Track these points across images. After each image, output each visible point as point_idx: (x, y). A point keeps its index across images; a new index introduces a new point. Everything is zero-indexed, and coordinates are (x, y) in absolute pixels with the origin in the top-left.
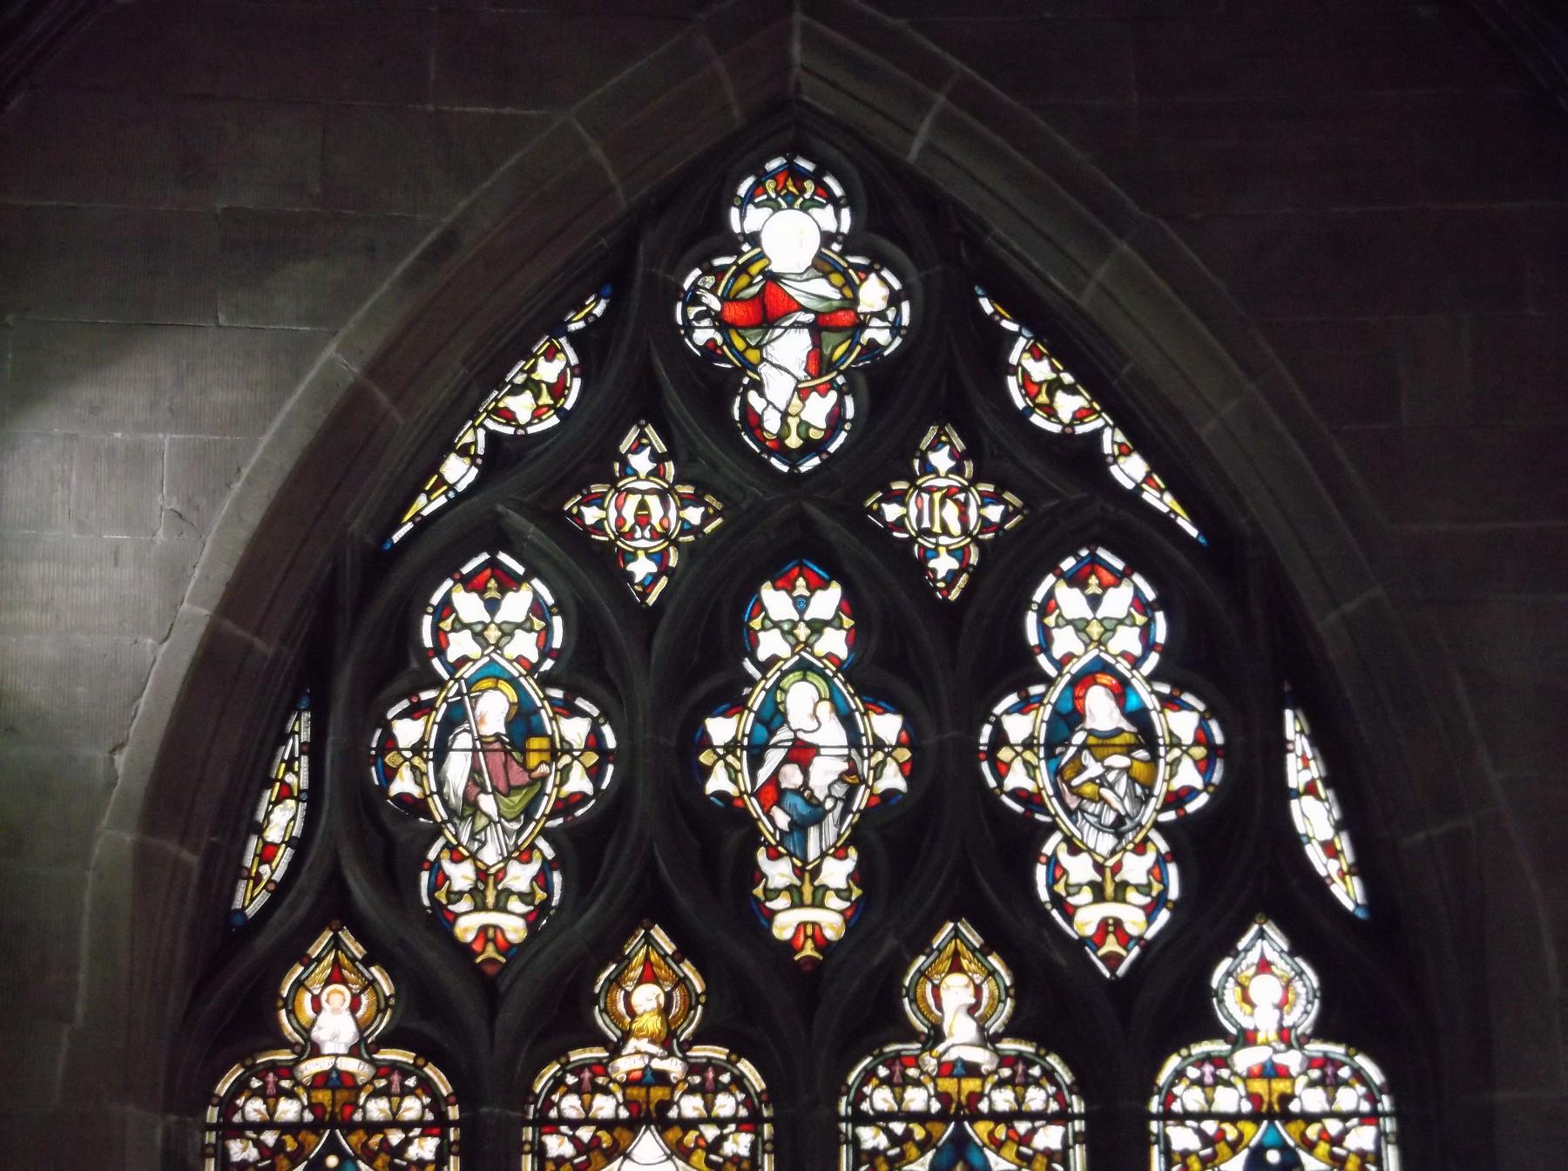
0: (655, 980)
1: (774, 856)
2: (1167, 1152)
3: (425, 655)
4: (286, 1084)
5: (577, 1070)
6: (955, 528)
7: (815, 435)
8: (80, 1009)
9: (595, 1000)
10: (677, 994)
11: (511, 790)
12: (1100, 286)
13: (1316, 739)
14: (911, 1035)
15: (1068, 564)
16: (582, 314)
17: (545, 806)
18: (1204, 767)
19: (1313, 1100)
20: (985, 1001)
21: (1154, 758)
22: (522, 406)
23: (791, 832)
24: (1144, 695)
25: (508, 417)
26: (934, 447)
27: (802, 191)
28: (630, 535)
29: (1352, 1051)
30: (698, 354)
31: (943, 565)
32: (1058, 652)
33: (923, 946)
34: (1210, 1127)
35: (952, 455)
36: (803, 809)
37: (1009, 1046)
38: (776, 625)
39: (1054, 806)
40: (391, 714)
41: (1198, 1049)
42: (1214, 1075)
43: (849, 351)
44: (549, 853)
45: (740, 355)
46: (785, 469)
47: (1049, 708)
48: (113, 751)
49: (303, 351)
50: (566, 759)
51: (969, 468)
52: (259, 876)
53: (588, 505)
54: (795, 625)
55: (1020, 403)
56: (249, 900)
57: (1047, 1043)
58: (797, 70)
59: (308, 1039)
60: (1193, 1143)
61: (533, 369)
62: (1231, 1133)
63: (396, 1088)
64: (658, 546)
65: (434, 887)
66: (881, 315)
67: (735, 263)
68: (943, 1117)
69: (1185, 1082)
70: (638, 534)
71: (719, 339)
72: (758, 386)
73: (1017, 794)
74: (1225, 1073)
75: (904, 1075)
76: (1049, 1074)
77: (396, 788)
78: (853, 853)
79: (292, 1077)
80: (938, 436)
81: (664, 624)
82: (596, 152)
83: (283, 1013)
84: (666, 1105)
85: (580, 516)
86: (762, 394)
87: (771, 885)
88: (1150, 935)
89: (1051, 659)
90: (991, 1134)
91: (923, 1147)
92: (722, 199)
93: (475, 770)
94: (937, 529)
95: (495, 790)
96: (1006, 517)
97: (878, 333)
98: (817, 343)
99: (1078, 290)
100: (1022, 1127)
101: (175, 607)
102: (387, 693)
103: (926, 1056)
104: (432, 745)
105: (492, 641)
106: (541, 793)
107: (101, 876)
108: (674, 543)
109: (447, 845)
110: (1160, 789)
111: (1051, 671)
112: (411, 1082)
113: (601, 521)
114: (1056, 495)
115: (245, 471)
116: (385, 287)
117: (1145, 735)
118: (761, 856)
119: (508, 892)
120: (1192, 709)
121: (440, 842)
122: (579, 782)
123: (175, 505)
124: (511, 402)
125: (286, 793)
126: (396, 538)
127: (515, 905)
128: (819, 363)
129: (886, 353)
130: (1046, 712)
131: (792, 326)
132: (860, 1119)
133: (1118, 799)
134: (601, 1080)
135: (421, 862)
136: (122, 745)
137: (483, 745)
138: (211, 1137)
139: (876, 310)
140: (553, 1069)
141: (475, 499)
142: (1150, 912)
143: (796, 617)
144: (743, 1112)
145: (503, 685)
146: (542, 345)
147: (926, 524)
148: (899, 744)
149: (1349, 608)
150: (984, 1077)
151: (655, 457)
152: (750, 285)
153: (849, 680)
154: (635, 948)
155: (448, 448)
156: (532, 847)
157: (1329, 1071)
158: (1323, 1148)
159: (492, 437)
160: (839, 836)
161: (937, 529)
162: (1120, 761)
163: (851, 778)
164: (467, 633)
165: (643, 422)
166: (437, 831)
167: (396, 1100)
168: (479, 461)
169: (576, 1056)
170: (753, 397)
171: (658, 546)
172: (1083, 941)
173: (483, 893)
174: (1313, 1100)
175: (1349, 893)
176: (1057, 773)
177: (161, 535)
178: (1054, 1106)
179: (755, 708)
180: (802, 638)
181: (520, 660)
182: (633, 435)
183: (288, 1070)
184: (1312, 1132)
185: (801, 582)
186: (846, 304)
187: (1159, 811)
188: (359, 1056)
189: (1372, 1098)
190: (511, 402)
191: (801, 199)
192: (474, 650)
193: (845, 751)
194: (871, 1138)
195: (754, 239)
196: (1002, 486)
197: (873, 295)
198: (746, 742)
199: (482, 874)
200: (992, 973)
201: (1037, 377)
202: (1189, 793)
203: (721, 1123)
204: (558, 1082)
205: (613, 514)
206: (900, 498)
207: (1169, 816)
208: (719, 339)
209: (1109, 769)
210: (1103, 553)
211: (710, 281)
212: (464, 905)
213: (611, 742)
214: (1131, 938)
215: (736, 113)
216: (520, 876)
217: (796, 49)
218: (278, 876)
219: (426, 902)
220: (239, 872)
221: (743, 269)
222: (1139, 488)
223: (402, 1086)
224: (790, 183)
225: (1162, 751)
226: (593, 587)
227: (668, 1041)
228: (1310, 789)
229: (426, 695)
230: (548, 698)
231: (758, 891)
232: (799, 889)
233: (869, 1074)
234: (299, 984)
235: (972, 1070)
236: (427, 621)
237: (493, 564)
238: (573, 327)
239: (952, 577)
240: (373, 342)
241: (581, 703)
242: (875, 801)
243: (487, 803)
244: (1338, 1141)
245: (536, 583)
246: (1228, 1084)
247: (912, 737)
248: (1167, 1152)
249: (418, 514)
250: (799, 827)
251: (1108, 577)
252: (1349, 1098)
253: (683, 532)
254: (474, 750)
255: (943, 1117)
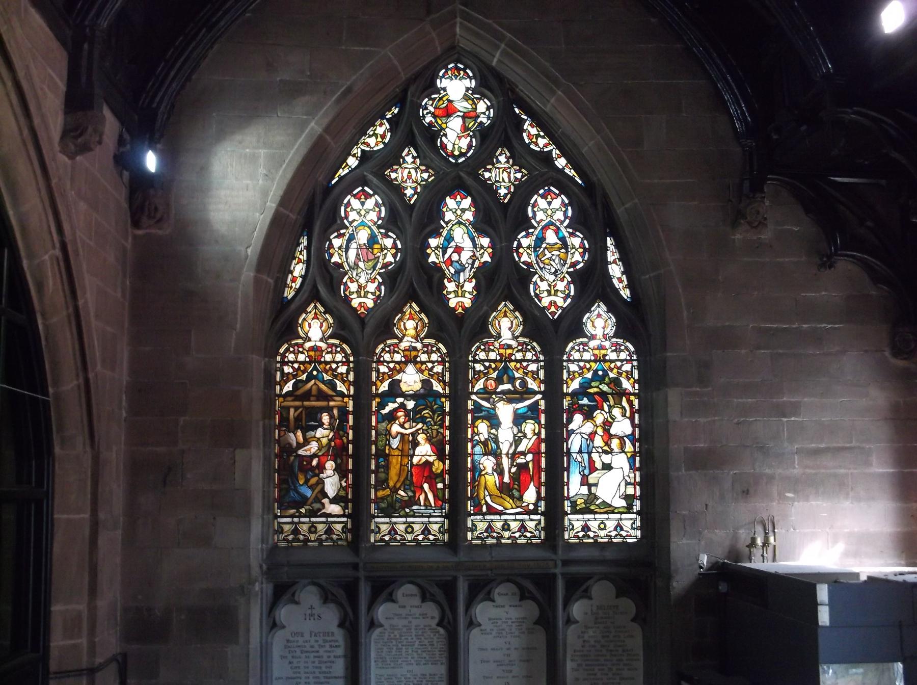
0: (413, 319)
1: (450, 281)
2: (569, 372)
3: (342, 219)
4: (301, 349)
5: (389, 347)
6: (507, 180)
7: (463, 151)
8: (238, 326)
9: (395, 325)
10: (420, 323)
11: (369, 260)
12: (553, 106)
13: (616, 246)
14: (492, 336)
15: (541, 191)
16: (391, 113)
17: (379, 266)
18: (582, 255)
19: (613, 356)
20: (514, 326)
21: (567, 252)
22: (372, 141)
23: (455, 274)
24: (564, 232)
25: (368, 145)
26: (500, 155)
27: (460, 74)
28: (406, 182)
29: (625, 341)
31: (503, 191)
32: (538, 219)
33: (495, 309)
34: (582, 364)
35: (506, 157)
36: (459, 267)
37: (521, 339)
38: (451, 210)
39: (536, 266)
40: (331, 237)
41: (578, 341)
42: (583, 348)
43: (474, 124)
44: (381, 280)
45: (440, 126)
46: (454, 161)
47: (535, 236)
48: (247, 248)
49: (303, 125)
50: (385, 251)
51: (511, 161)
52: (292, 287)
53: (392, 172)
54: (456, 210)
55: (527, 141)
56: (289, 294)
57: (533, 339)
58: (458, 36)
59: (307, 336)
60: (577, 369)
61: (375, 130)
62: (588, 366)
63: (334, 351)
64: (414, 185)
65: (345, 290)
66: (484, 113)
68: (501, 361)
69: (575, 350)
70: (408, 181)
71: (434, 121)
72: (445, 135)
73: (524, 263)
74: (586, 348)
75: (489, 348)
76: (533, 348)
77: (333, 260)
78: (474, 281)
79: (303, 348)
80: (501, 151)
81: (416, 208)
82: (396, 62)
83: (299, 328)
84: (416, 357)
85: (390, 175)
86: (447, 138)
87: (449, 290)
88: (564, 306)
89: (536, 221)
90: (515, 366)
91: (494, 370)
92: (434, 77)
93: (358, 254)
94: (501, 180)
95: (364, 260)
96: (523, 177)
97: (483, 119)
98: (464, 122)
99: (545, 105)
100: (525, 364)
101: (265, 204)
102: (331, 230)
103: (496, 342)
104: (344, 247)
105: (363, 214)
106: (378, 262)
107: (244, 286)
108: (419, 184)
109: (349, 277)
110: (569, 261)
111: (536, 225)
112: (339, 349)
113: (396, 178)
114: (537, 170)
115: (287, 161)
116: (329, 104)
117: (565, 245)
118: (446, 281)
119: (368, 292)
120: (579, 237)
121: (347, 277)
122: (390, 258)
123: (265, 172)
124: (369, 140)
125: (300, 261)
126: (333, 182)
127: (370, 296)
128: (465, 128)
130: (534, 238)
132: (475, 361)
133: (556, 264)
134: (396, 349)
135: (341, 282)
136: (249, 246)
137: (360, 247)
138: (278, 365)
140: (382, 346)
141: (357, 170)
142: (565, 300)
143: (457, 208)
144: (440, 359)
145: (366, 228)
146: (378, 123)
147: (497, 179)
148: (489, 247)
149: (627, 206)
150: (513, 349)
151: (413, 157)
152: (443, 104)
153: (473, 227)
154: (407, 309)
155: (349, 154)
156: (375, 278)
157: (618, 347)
158: (615, 370)
159: (363, 151)
160: (470, 275)
161: (501, 180)
162: (557, 253)
163: (474, 258)
164: (355, 212)
166: (346, 273)
167: (334, 355)
168: (359, 159)
169: (389, 342)
170: (444, 138)
171: (414, 185)
172: (544, 308)
173: (360, 292)
174: (613, 356)
175: (626, 294)
176: (538, 256)
177: (261, 182)
178: (534, 358)
179: (444, 236)
180: (459, 214)
181: (371, 220)
182: (406, 150)
183: (301, 346)
184: (612, 365)
185: (458, 197)
187: (568, 268)
188: (323, 342)
189: (630, 355)
190: (369, 140)
192: (357, 217)
193: (472, 249)
194: (479, 367)
195: (444, 89)
196: (521, 167)
197: (482, 107)
198: (441, 246)
199: (360, 287)
200: (516, 317)
201: (532, 133)
202: (578, 262)
203: (433, 362)
204: (383, 350)
205: (400, 175)
206: (490, 171)
207: (572, 270)
208: (434, 121)
209: (553, 255)
210: (552, 188)
211: (431, 102)
212: (355, 296)
213: (399, 246)
214: (559, 307)
215: (439, 49)
216: (372, 287)
217: (458, 30)
218: (297, 287)
219: (343, 295)
220: (285, 285)
221: (441, 99)
222: (563, 168)
223: (336, 350)
225: (569, 250)
226: (394, 197)
227: (416, 337)
228: (614, 262)
229: (342, 231)
230: (380, 232)
231: (445, 292)
232: (457, 291)
233: (478, 348)
234: (304, 319)
235: (510, 347)
236: (343, 208)
237: (363, 190)
238: (388, 117)
239: (506, 195)
240: (326, 121)
241: (390, 234)
242: (481, 264)
243: (361, 264)
244: (620, 368)
245: (376, 196)
246: (587, 351)
247: (493, 245)
248: (569, 372)
249: (340, 175)
250: (458, 272)
251: (553, 196)
252: (623, 356)
253: (422, 181)
254: (357, 248)
255: (501, 361)
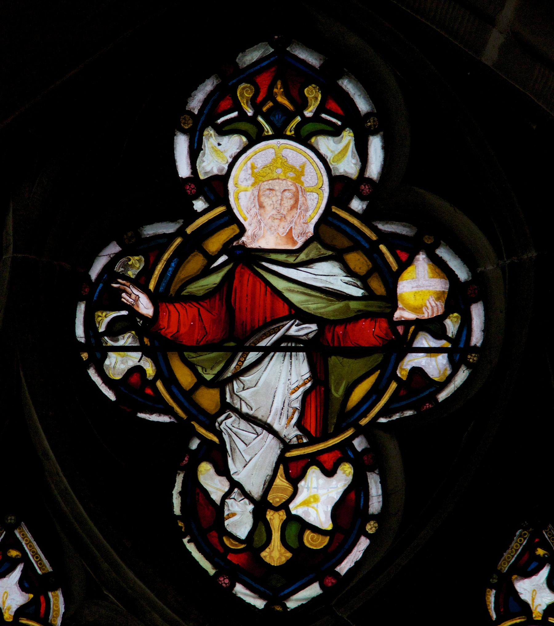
30: (111, 396)
67: (181, 232)
71: (150, 369)
80: (530, 548)
129: (442, 396)
131: (276, 347)
139: (426, 315)
152: (206, 272)
165: (11, 519)
186: (374, 306)
191: (299, 119)
208: (150, 369)
224: (278, 89)
